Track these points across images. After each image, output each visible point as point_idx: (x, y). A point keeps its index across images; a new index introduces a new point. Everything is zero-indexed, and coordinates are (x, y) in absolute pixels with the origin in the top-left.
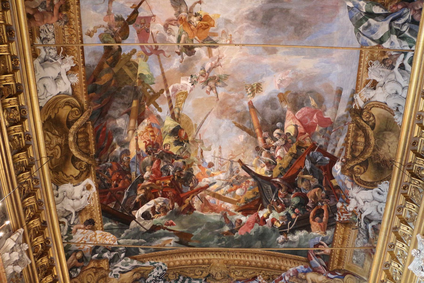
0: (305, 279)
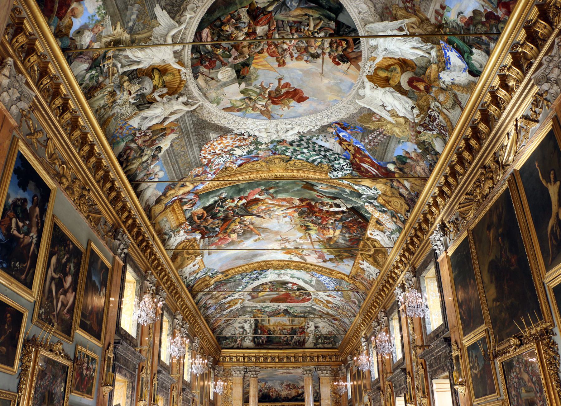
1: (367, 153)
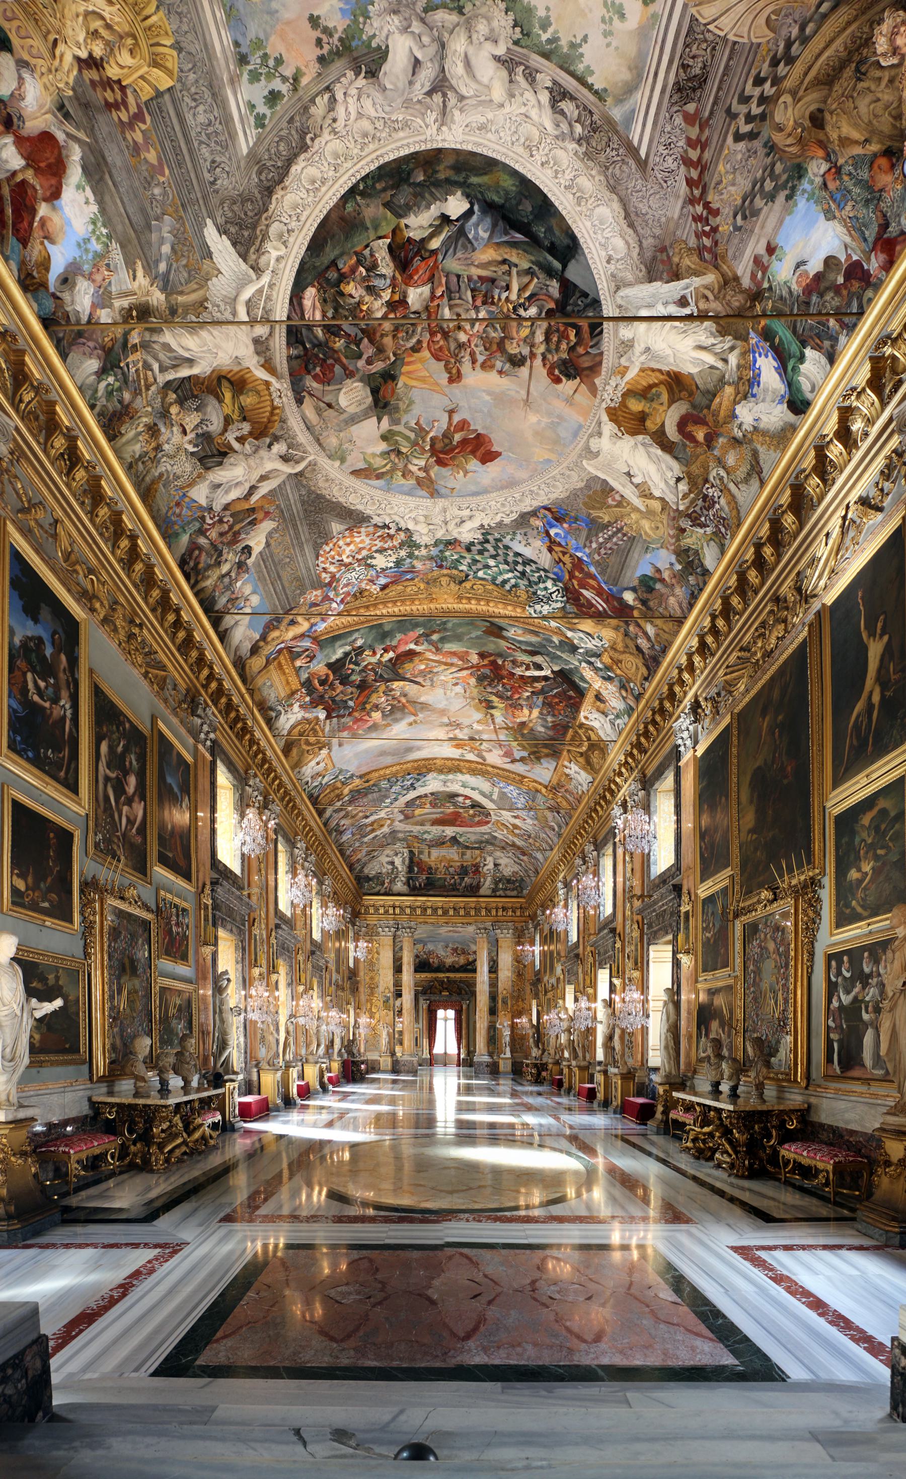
0: (308, 620)
1: (593, 569)
